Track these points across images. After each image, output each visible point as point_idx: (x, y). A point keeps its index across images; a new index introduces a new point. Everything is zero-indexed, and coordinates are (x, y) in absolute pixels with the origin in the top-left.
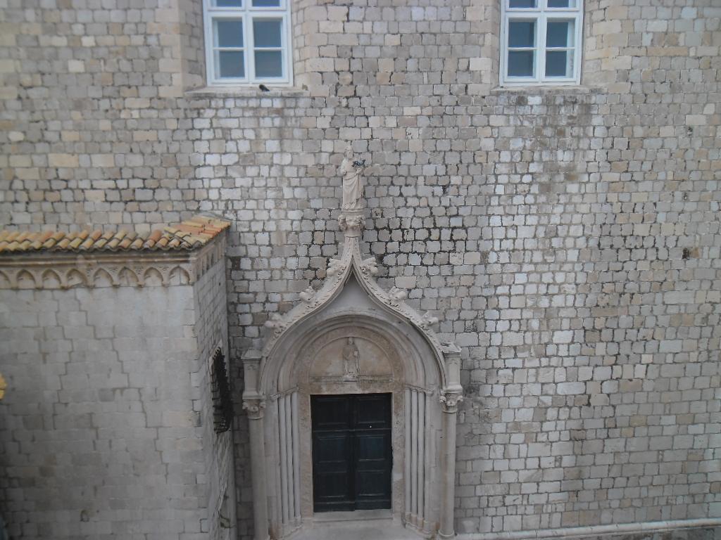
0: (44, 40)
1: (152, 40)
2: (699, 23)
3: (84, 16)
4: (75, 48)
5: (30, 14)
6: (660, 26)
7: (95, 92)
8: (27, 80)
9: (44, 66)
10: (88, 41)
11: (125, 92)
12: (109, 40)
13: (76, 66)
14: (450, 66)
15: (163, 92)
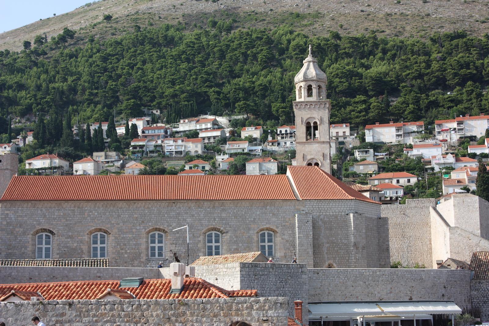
0: (120, 251)
1: (140, 251)
2: (243, 246)
3: (128, 247)
4: (126, 253)
5: (118, 247)
6: (235, 247)
7: (129, 260)
8: (117, 258)
9: (120, 256)
10: (128, 251)
11: (134, 260)
12: (132, 251)
13: (126, 256)
14: (195, 255)
15: (141, 260)
